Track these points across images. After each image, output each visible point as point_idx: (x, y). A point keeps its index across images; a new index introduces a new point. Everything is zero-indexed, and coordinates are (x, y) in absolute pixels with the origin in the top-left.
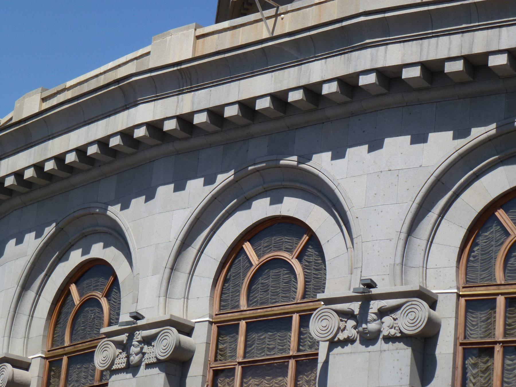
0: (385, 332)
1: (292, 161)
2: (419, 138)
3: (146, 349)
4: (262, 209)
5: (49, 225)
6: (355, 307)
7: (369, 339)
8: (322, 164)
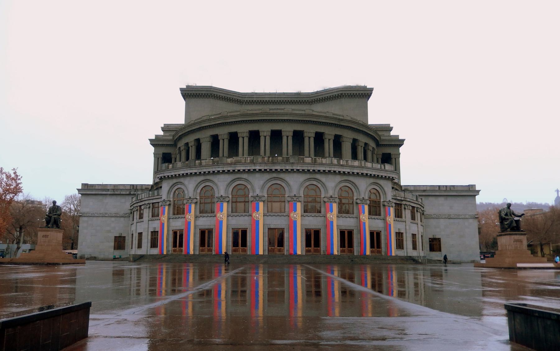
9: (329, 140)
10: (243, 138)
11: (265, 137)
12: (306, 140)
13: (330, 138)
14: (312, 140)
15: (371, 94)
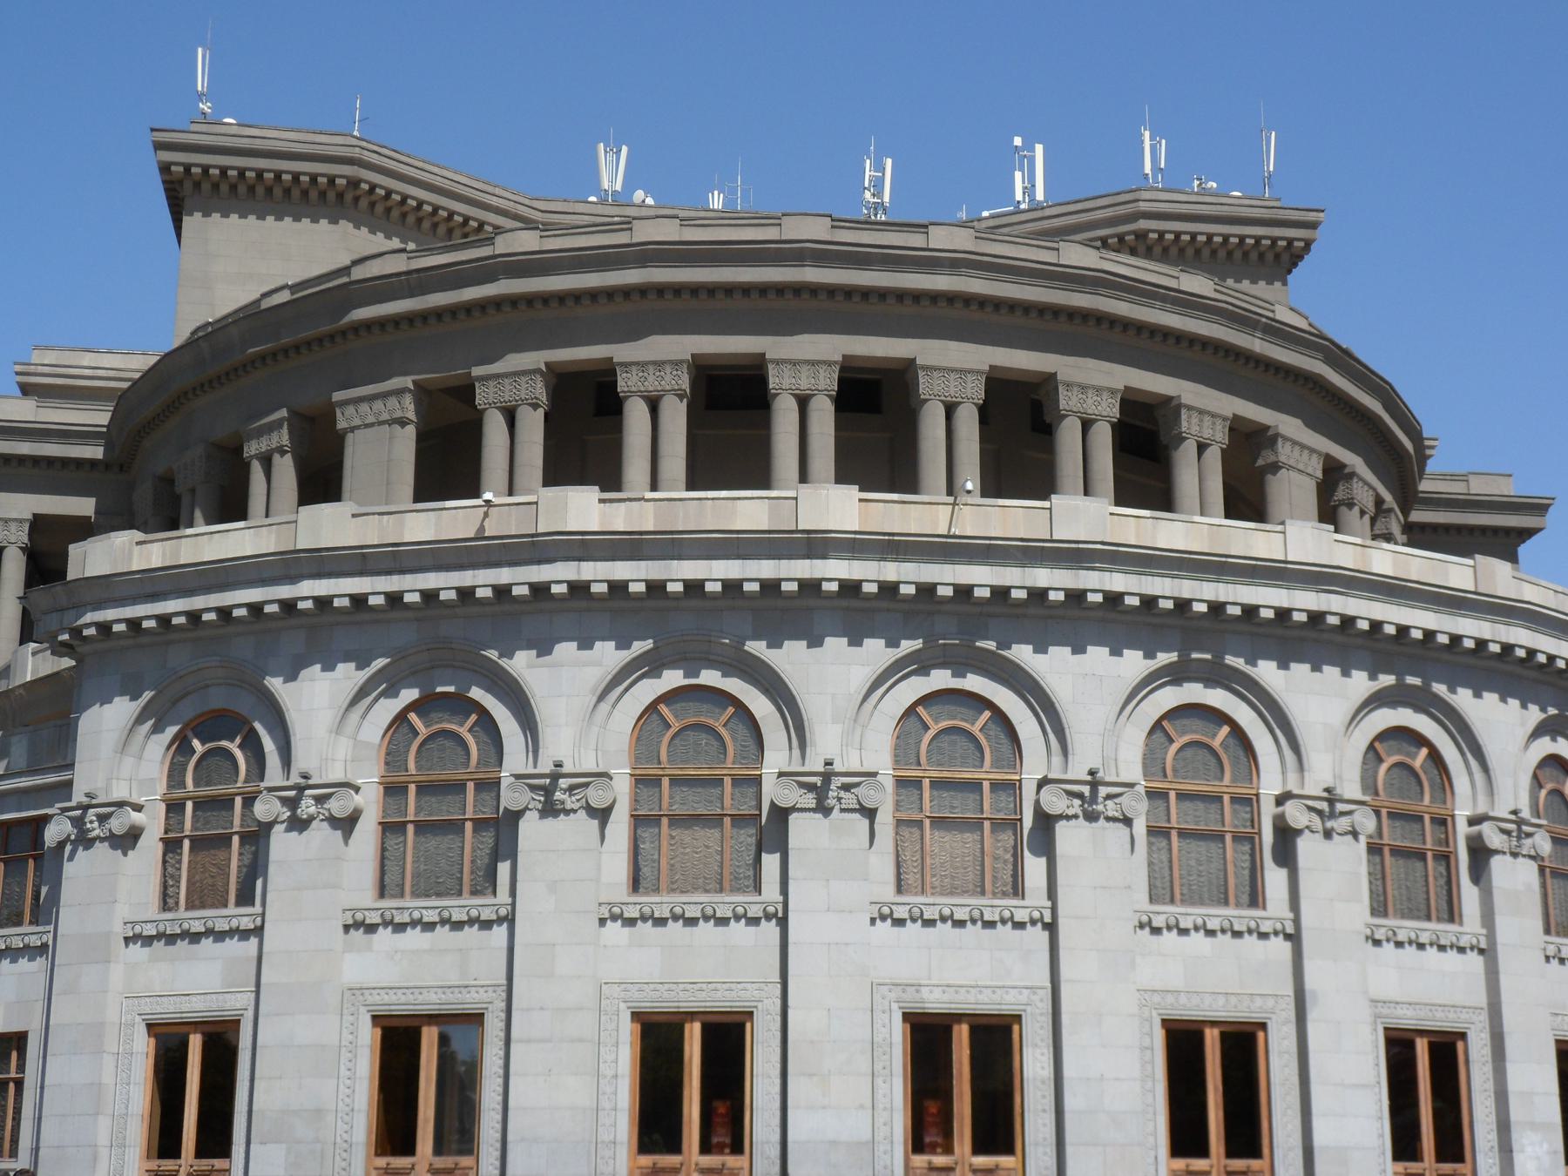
0: (1110, 814)
1: (990, 645)
2: (1116, 652)
3: (842, 794)
4: (941, 679)
5: (644, 639)
6: (1086, 790)
7: (1091, 817)
8: (1022, 653)
9: (1202, 448)
10: (654, 405)
11: (803, 402)
12: (1069, 436)
13: (1207, 433)
14: (1103, 438)
15: (1308, 244)
